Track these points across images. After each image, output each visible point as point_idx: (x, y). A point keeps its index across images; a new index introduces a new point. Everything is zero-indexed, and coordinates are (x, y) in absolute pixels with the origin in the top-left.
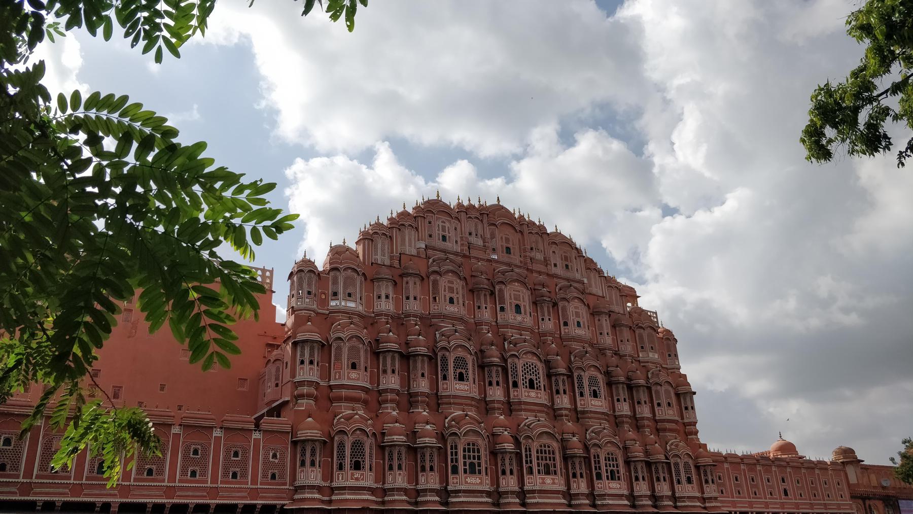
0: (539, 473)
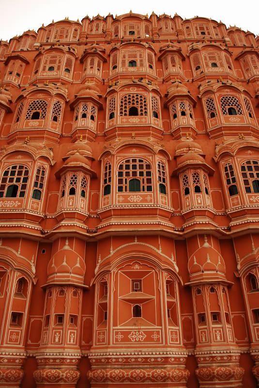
0: (120, 189)
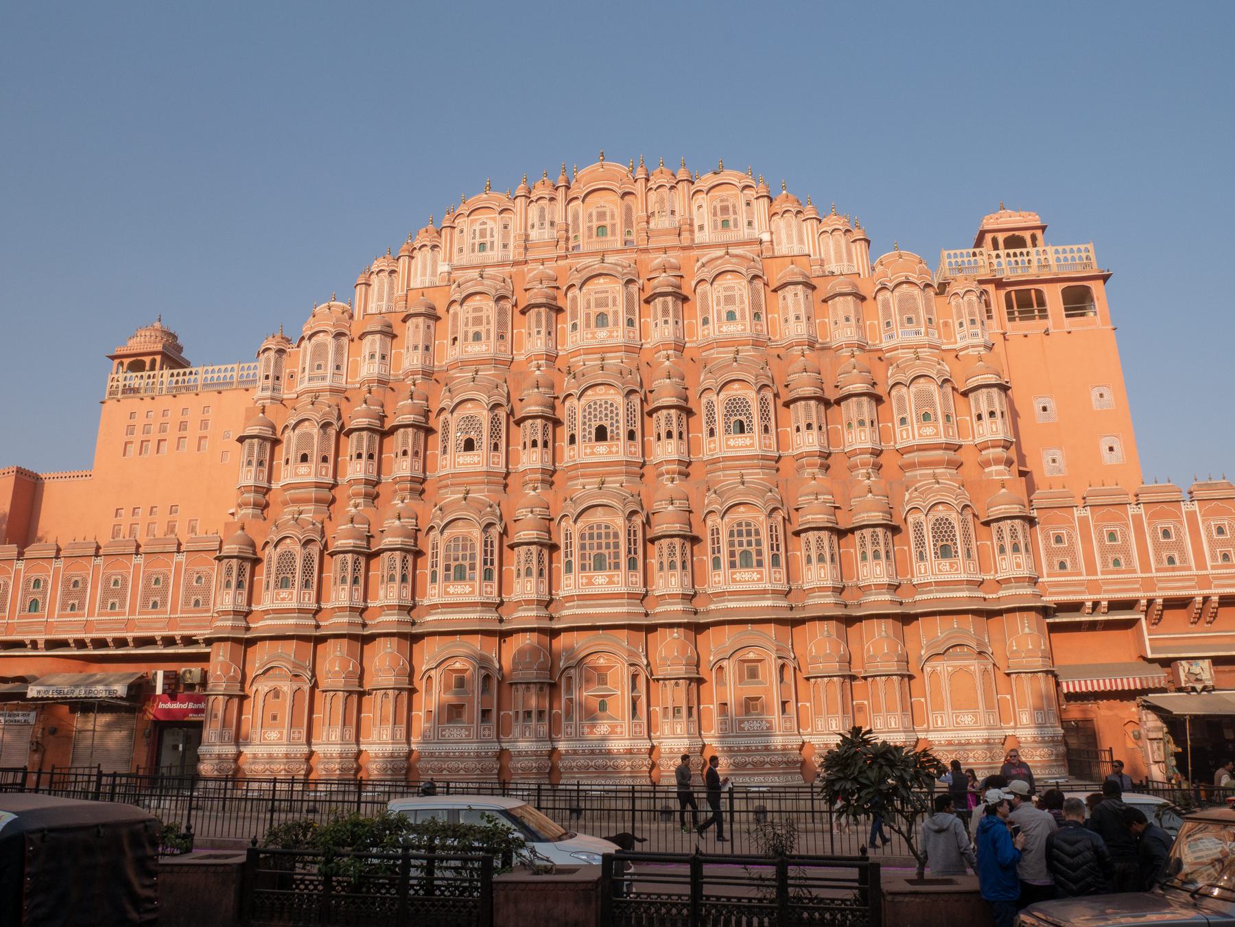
0: (583, 568)
